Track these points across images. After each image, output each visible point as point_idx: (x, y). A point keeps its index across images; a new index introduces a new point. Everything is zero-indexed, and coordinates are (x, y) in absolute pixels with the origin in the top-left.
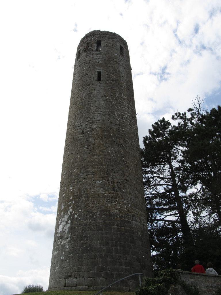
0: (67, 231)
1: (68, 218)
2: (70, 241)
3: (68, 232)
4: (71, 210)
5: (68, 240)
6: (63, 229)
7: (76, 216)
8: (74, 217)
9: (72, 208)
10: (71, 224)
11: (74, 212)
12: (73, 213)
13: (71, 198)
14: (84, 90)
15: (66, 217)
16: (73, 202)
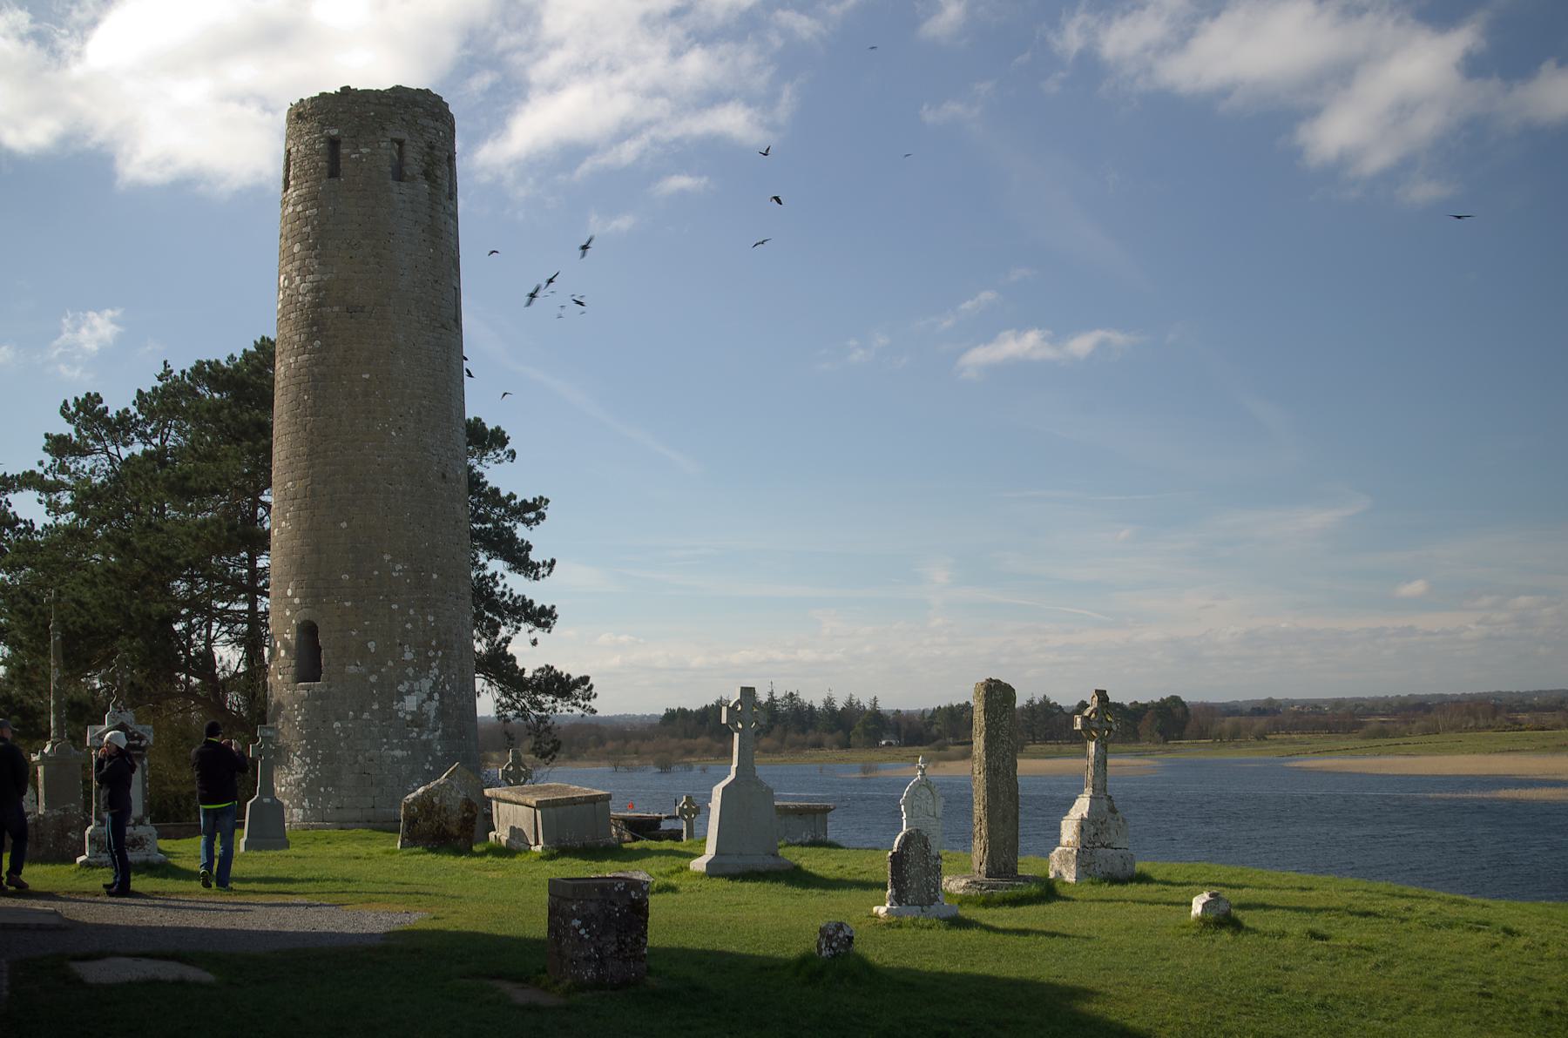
0: (433, 714)
1: (430, 688)
2: (441, 738)
3: (434, 718)
4: (436, 671)
5: (437, 733)
6: (420, 707)
7: (448, 687)
8: (444, 687)
9: (437, 667)
10: (441, 702)
11: (443, 677)
12: (441, 680)
13: (434, 643)
14: (435, 335)
15: (427, 684)
16: (440, 653)
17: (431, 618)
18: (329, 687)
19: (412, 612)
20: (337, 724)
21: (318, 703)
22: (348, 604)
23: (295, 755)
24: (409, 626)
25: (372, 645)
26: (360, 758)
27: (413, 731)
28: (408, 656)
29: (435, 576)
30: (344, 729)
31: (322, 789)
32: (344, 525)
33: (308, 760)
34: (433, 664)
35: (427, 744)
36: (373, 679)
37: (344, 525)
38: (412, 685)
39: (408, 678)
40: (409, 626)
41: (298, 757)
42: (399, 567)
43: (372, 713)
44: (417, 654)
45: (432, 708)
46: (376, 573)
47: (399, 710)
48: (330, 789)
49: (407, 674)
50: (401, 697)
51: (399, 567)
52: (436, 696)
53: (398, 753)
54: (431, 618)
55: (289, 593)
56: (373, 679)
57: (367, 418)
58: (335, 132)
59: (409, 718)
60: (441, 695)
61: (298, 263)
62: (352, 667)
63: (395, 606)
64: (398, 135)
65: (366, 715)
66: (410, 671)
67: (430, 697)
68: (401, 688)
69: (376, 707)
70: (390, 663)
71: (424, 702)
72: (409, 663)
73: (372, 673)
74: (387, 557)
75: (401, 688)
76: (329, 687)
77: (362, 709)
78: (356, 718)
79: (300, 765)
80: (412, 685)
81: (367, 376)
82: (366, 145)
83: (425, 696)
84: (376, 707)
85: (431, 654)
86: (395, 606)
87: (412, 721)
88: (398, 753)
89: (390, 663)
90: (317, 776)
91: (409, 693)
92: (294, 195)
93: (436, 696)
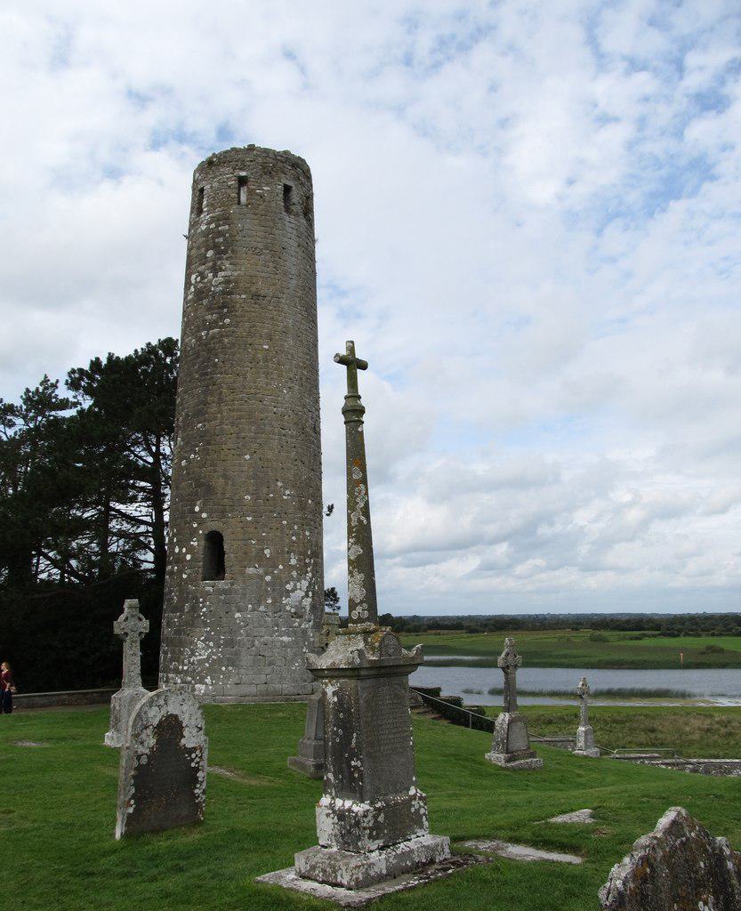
2: (313, 626)
4: (310, 574)
6: (301, 602)
8: (314, 588)
15: (305, 584)
17: (307, 533)
18: (232, 584)
19: (296, 527)
20: (238, 615)
21: (222, 597)
22: (249, 519)
23: (199, 640)
24: (294, 538)
25: (267, 552)
26: (256, 642)
27: (295, 622)
28: (293, 562)
29: (310, 502)
30: (244, 619)
31: (224, 668)
32: (248, 457)
33: (211, 644)
34: (309, 569)
35: (304, 632)
36: (268, 578)
37: (248, 457)
38: (295, 585)
39: (292, 578)
40: (294, 538)
41: (202, 641)
42: (287, 492)
43: (266, 607)
44: (299, 560)
45: (307, 602)
46: (271, 495)
47: (286, 604)
48: (230, 668)
49: (292, 576)
50: (288, 594)
51: (287, 492)
52: (310, 593)
53: (285, 639)
54: (307, 533)
55: (197, 509)
56: (268, 578)
57: (267, 378)
58: (243, 174)
59: (293, 610)
60: (313, 592)
61: (211, 264)
62: (251, 569)
63: (285, 522)
64: (289, 183)
65: (262, 608)
66: (294, 573)
67: (307, 596)
68: (289, 587)
69: (270, 601)
70: (281, 567)
71: (303, 598)
72: (293, 567)
73: (267, 574)
74: (280, 484)
75: (289, 587)
76: (232, 584)
77: (259, 602)
78: (253, 610)
79: (203, 649)
80: (295, 585)
81: (266, 347)
82: (267, 185)
83: (303, 594)
84: (270, 601)
85: (307, 561)
86: (285, 522)
87: (295, 613)
88: (285, 639)
89: (281, 567)
90: (219, 657)
91: (293, 591)
92: (208, 217)
93: (310, 593)
